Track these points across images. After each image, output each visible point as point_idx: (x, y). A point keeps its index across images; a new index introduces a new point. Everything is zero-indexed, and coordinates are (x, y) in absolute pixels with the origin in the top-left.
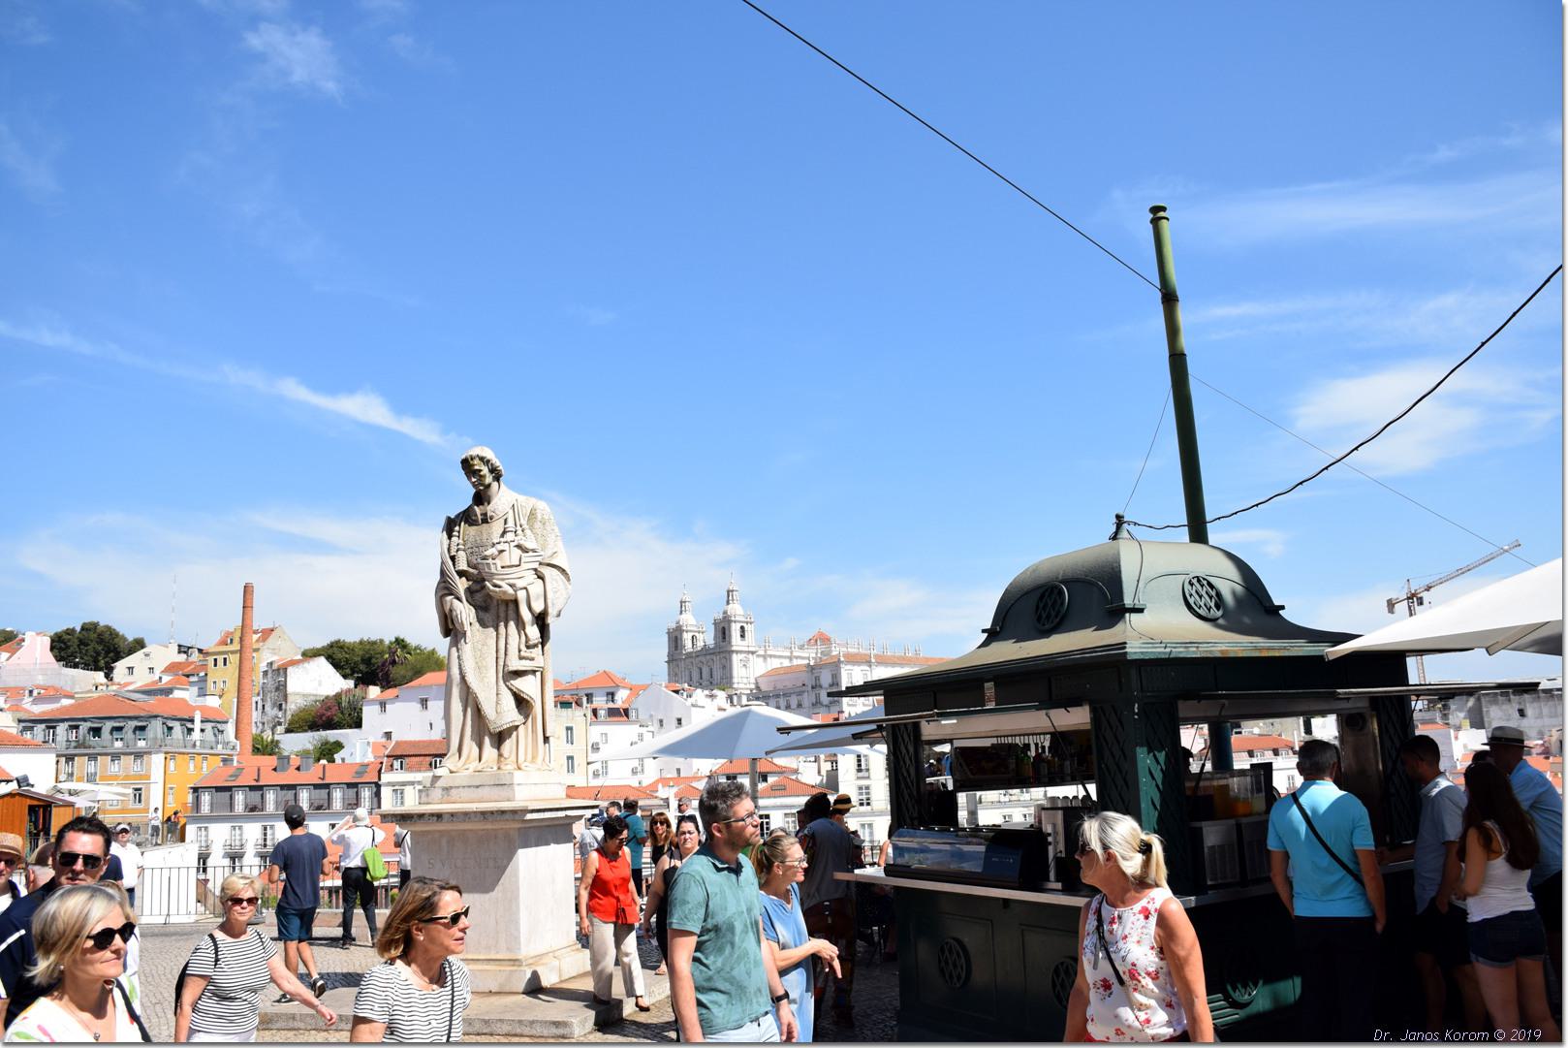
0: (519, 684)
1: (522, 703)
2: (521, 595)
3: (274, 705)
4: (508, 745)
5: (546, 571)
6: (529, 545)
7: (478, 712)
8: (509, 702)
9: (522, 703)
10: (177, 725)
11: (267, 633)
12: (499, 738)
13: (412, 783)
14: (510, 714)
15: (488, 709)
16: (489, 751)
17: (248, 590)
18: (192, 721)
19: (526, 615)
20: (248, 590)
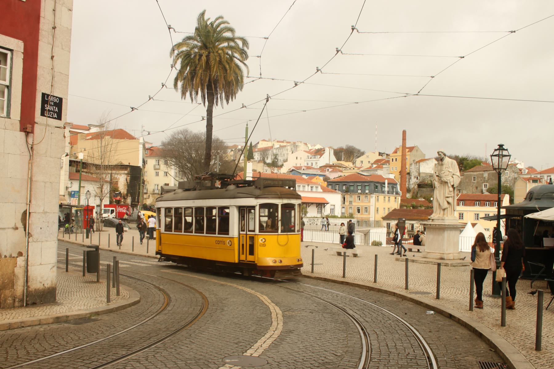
0: (448, 199)
1: (448, 203)
2: (448, 181)
3: (415, 177)
4: (446, 211)
5: (454, 176)
6: (450, 171)
7: (439, 204)
8: (446, 203)
9: (448, 203)
10: (379, 185)
11: (411, 149)
12: (444, 210)
13: (467, 211)
14: (446, 205)
15: (441, 204)
16: (442, 212)
17: (404, 133)
18: (384, 183)
19: (449, 185)
20: (404, 133)
